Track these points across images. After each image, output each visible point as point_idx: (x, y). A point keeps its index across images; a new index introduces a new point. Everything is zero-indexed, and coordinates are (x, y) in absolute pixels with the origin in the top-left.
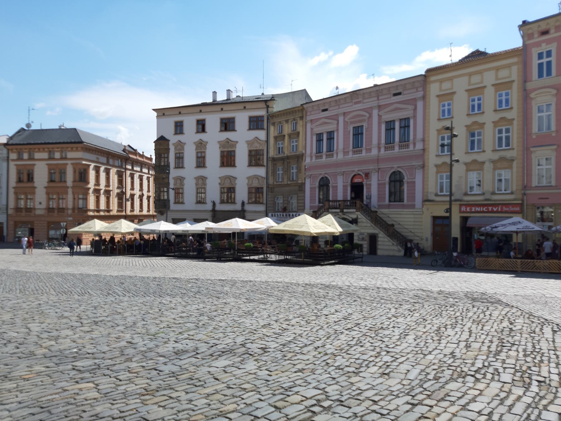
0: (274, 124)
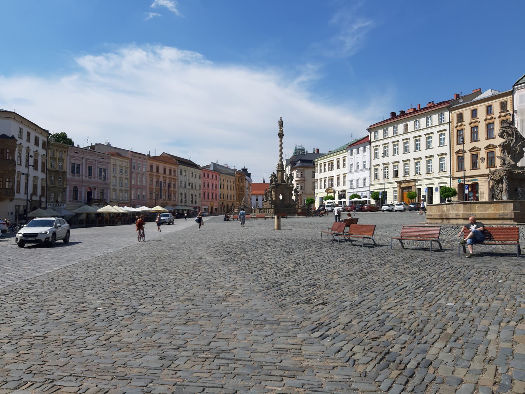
0: (50, 149)
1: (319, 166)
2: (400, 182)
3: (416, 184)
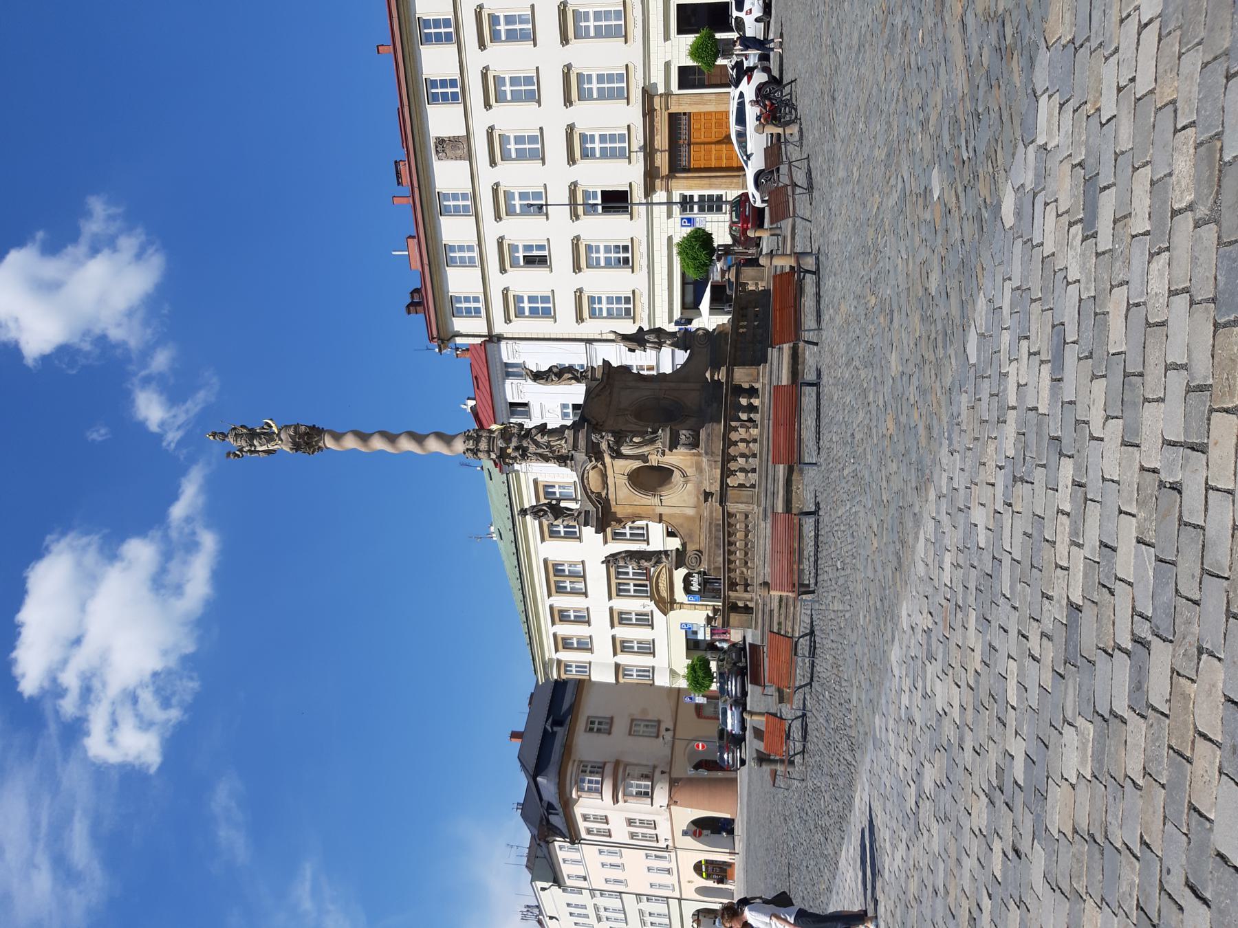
1: (565, 656)
2: (651, 175)
3: (661, 90)
